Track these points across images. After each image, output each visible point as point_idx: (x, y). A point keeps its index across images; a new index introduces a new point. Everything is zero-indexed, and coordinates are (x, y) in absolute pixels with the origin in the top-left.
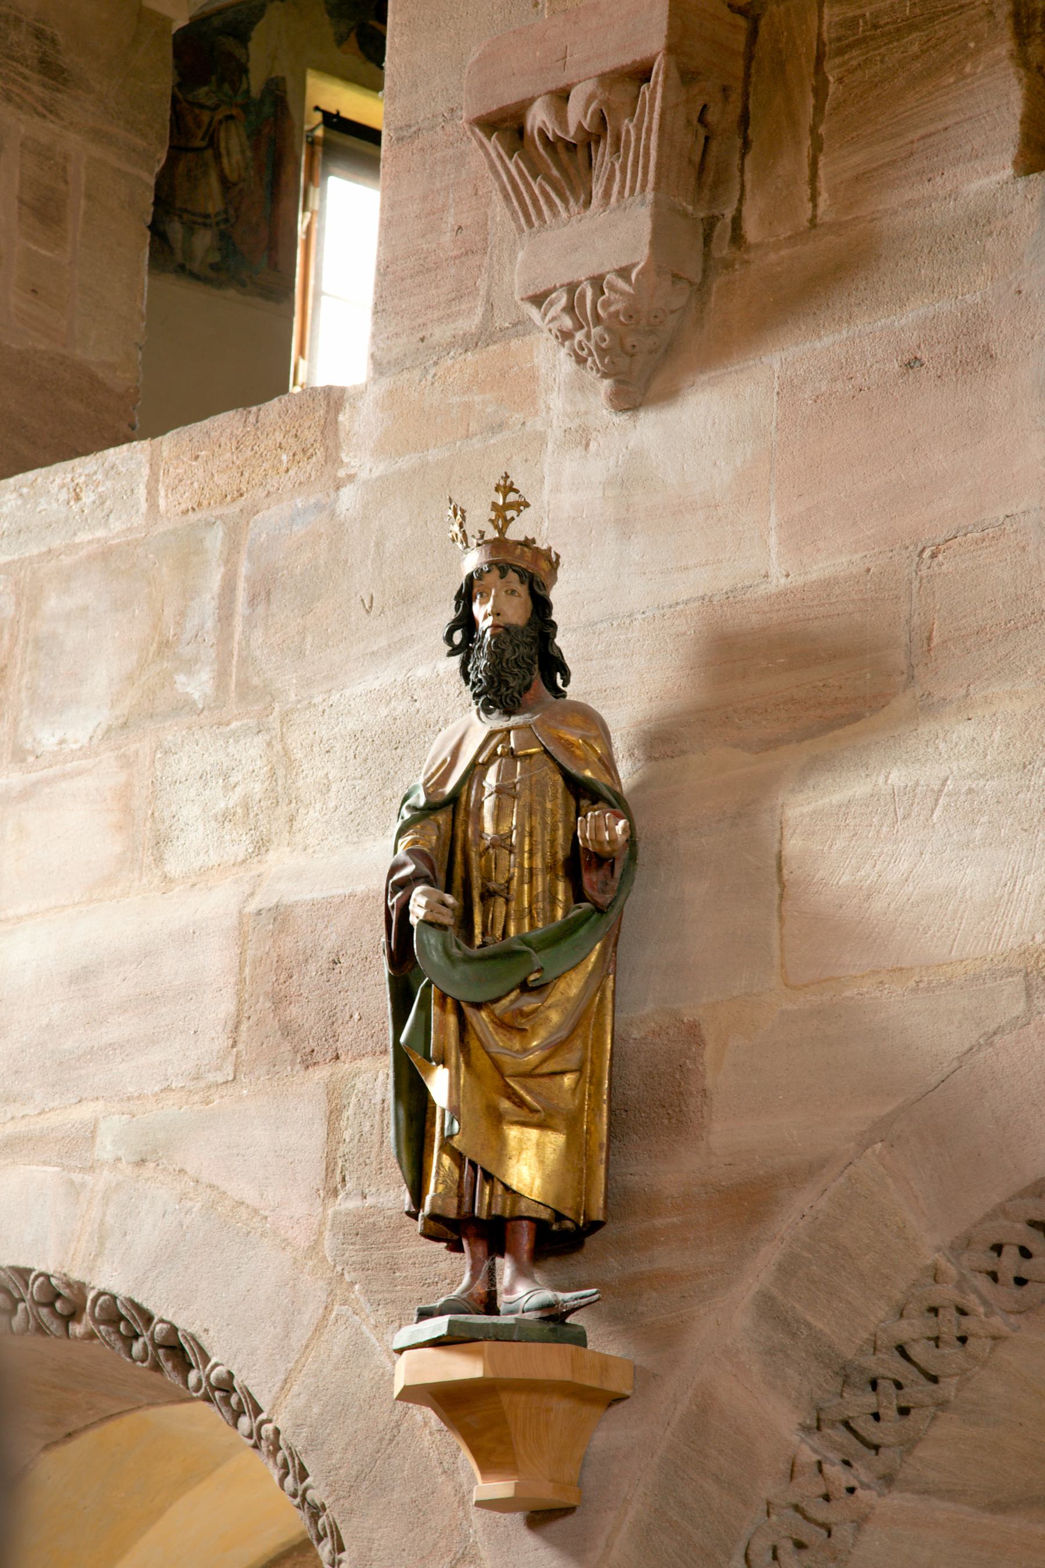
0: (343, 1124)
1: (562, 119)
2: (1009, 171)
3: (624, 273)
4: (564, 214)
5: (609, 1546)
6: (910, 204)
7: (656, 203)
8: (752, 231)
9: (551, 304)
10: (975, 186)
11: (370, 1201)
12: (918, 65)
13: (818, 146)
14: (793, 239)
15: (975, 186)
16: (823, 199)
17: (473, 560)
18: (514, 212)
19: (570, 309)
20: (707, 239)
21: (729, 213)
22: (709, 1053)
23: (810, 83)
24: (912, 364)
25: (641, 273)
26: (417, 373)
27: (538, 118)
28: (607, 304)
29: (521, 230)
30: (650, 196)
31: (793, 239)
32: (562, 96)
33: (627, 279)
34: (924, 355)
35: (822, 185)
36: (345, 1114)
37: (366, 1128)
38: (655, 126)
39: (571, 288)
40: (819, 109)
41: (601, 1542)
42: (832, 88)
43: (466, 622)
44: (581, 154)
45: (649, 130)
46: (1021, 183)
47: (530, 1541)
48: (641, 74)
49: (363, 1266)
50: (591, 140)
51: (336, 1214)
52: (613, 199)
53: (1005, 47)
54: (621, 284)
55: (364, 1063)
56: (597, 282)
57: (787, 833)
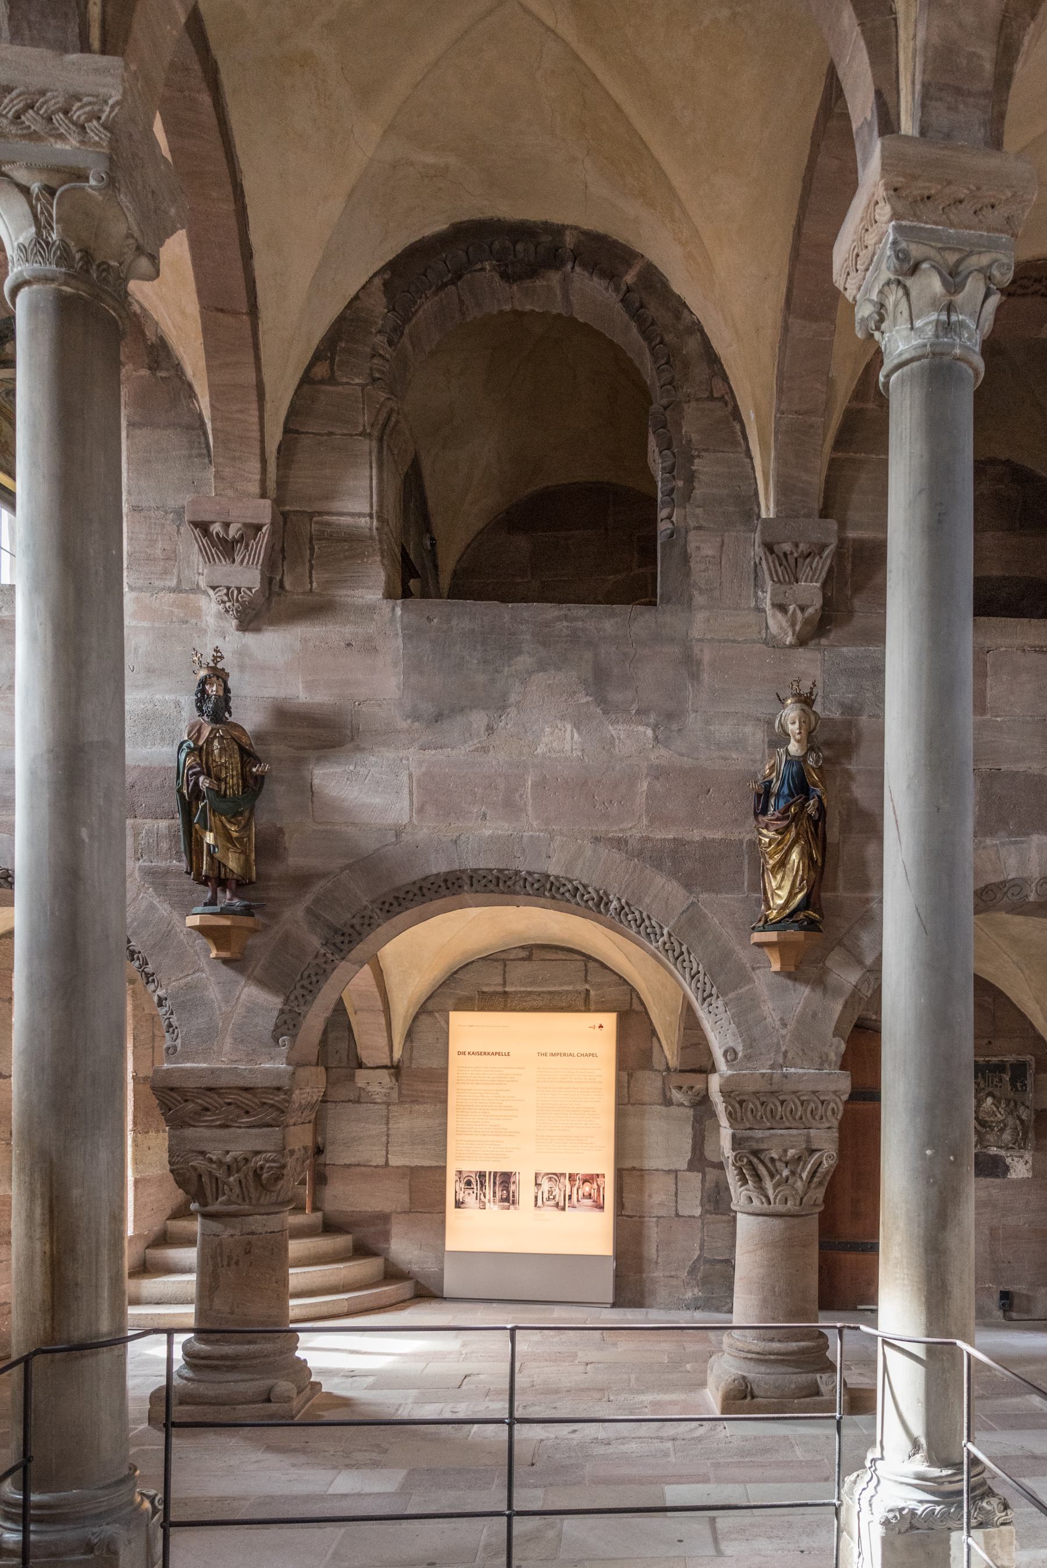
0: (140, 838)
1: (227, 532)
2: (381, 596)
3: (250, 589)
4: (224, 563)
5: (253, 971)
6: (346, 596)
7: (261, 570)
8: (288, 586)
9: (219, 591)
10: (369, 597)
11: (153, 864)
12: (347, 553)
13: (311, 567)
14: (303, 593)
15: (369, 597)
16: (314, 584)
17: (203, 673)
18: (203, 556)
19: (227, 594)
20: (270, 583)
21: (278, 578)
22: (286, 837)
23: (308, 546)
24: (349, 645)
25: (256, 591)
26: (149, 595)
27: (216, 528)
28: (242, 597)
29: (205, 562)
30: (259, 567)
31: (303, 593)
32: (226, 525)
33: (251, 592)
34: (354, 644)
35: (314, 579)
36: (141, 835)
37: (151, 841)
38: (264, 546)
39: (228, 588)
40: (312, 555)
41: (250, 969)
42: (316, 550)
43: (203, 691)
44: (230, 546)
45: (261, 546)
46: (385, 601)
47: (224, 967)
48: (258, 528)
49: (153, 883)
50: (235, 541)
51: (140, 866)
52: (245, 563)
53: (378, 559)
54: (248, 592)
55: (148, 820)
56: (239, 589)
57: (314, 777)
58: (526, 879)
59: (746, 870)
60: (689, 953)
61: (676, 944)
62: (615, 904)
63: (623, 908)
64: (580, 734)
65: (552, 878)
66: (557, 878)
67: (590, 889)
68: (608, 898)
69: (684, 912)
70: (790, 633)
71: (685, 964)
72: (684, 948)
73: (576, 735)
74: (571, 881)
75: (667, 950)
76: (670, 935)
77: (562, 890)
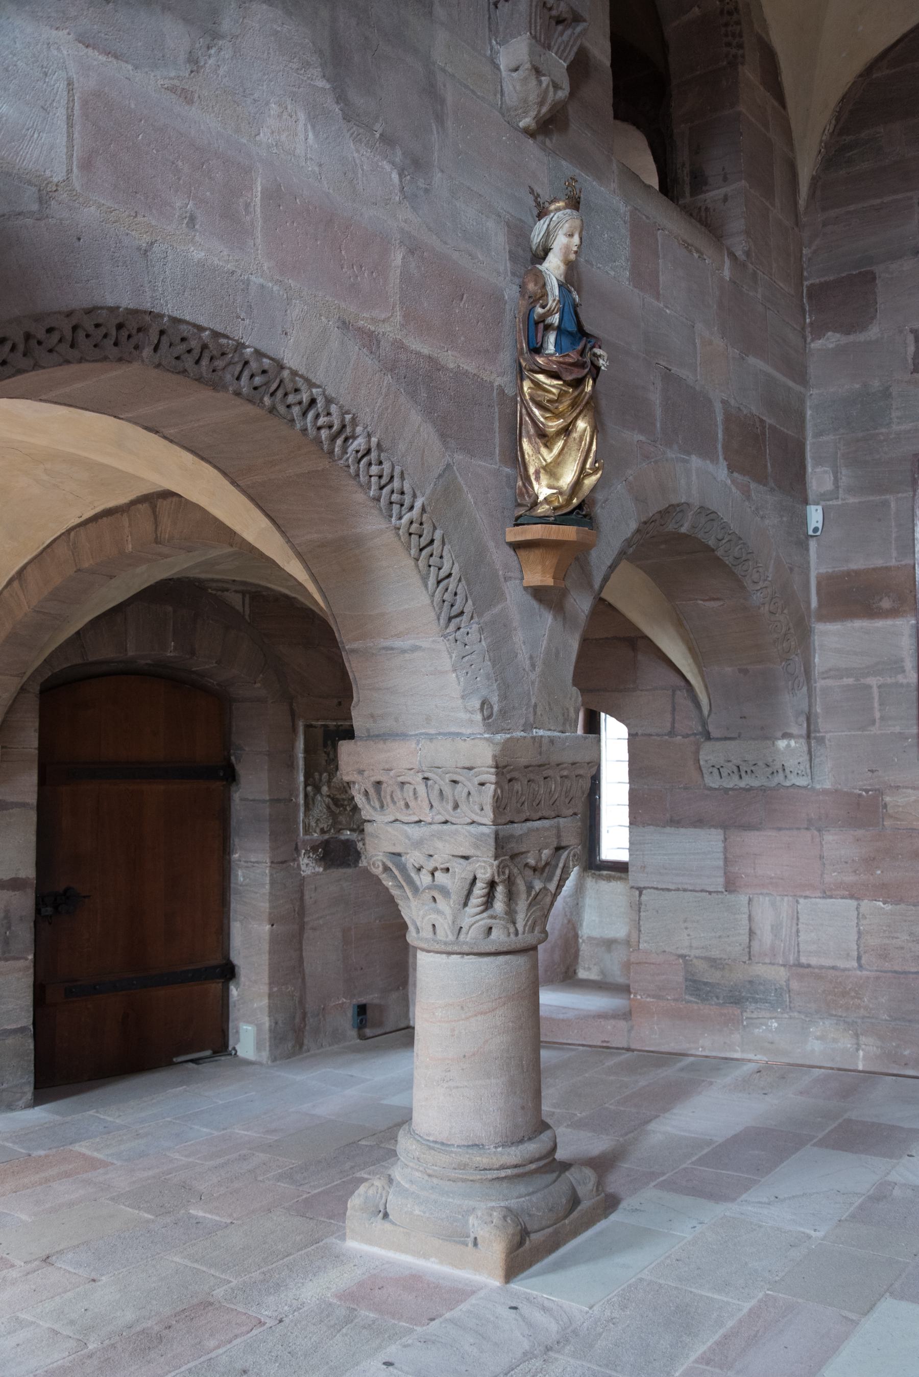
58: (246, 363)
59: (497, 430)
60: (443, 543)
61: (427, 528)
62: (359, 443)
63: (368, 452)
64: (316, 136)
65: (286, 373)
66: (294, 373)
67: (334, 408)
68: (354, 430)
69: (440, 476)
70: (533, 114)
71: (432, 561)
72: (438, 535)
73: (311, 136)
74: (311, 384)
75: (410, 534)
76: (423, 510)
77: (291, 399)
